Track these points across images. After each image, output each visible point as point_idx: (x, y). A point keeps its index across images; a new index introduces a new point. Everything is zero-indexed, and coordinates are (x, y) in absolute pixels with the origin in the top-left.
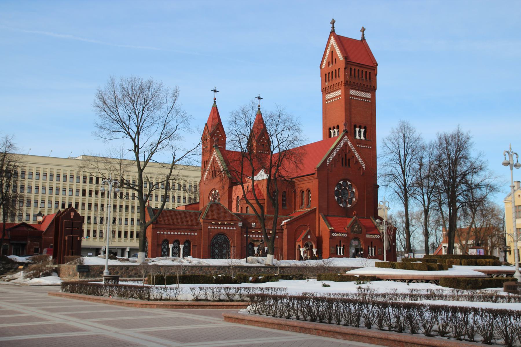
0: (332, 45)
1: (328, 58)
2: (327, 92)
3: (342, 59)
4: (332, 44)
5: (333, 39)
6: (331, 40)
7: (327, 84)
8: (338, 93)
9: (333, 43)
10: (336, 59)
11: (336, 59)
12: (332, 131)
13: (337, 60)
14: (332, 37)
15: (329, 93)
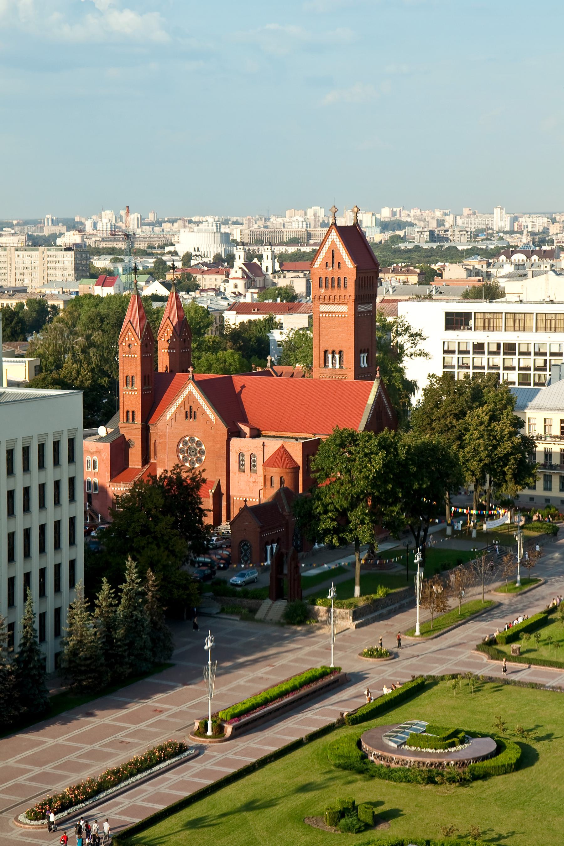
0: (333, 242)
1: (325, 256)
2: (322, 302)
3: (352, 267)
4: (333, 242)
5: (335, 234)
6: (332, 234)
7: (323, 291)
8: (343, 308)
9: (335, 240)
10: (339, 263)
11: (339, 263)
12: (330, 356)
13: (341, 265)
14: (333, 231)
15: (327, 304)
